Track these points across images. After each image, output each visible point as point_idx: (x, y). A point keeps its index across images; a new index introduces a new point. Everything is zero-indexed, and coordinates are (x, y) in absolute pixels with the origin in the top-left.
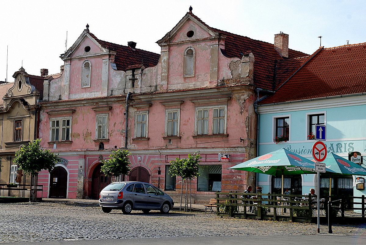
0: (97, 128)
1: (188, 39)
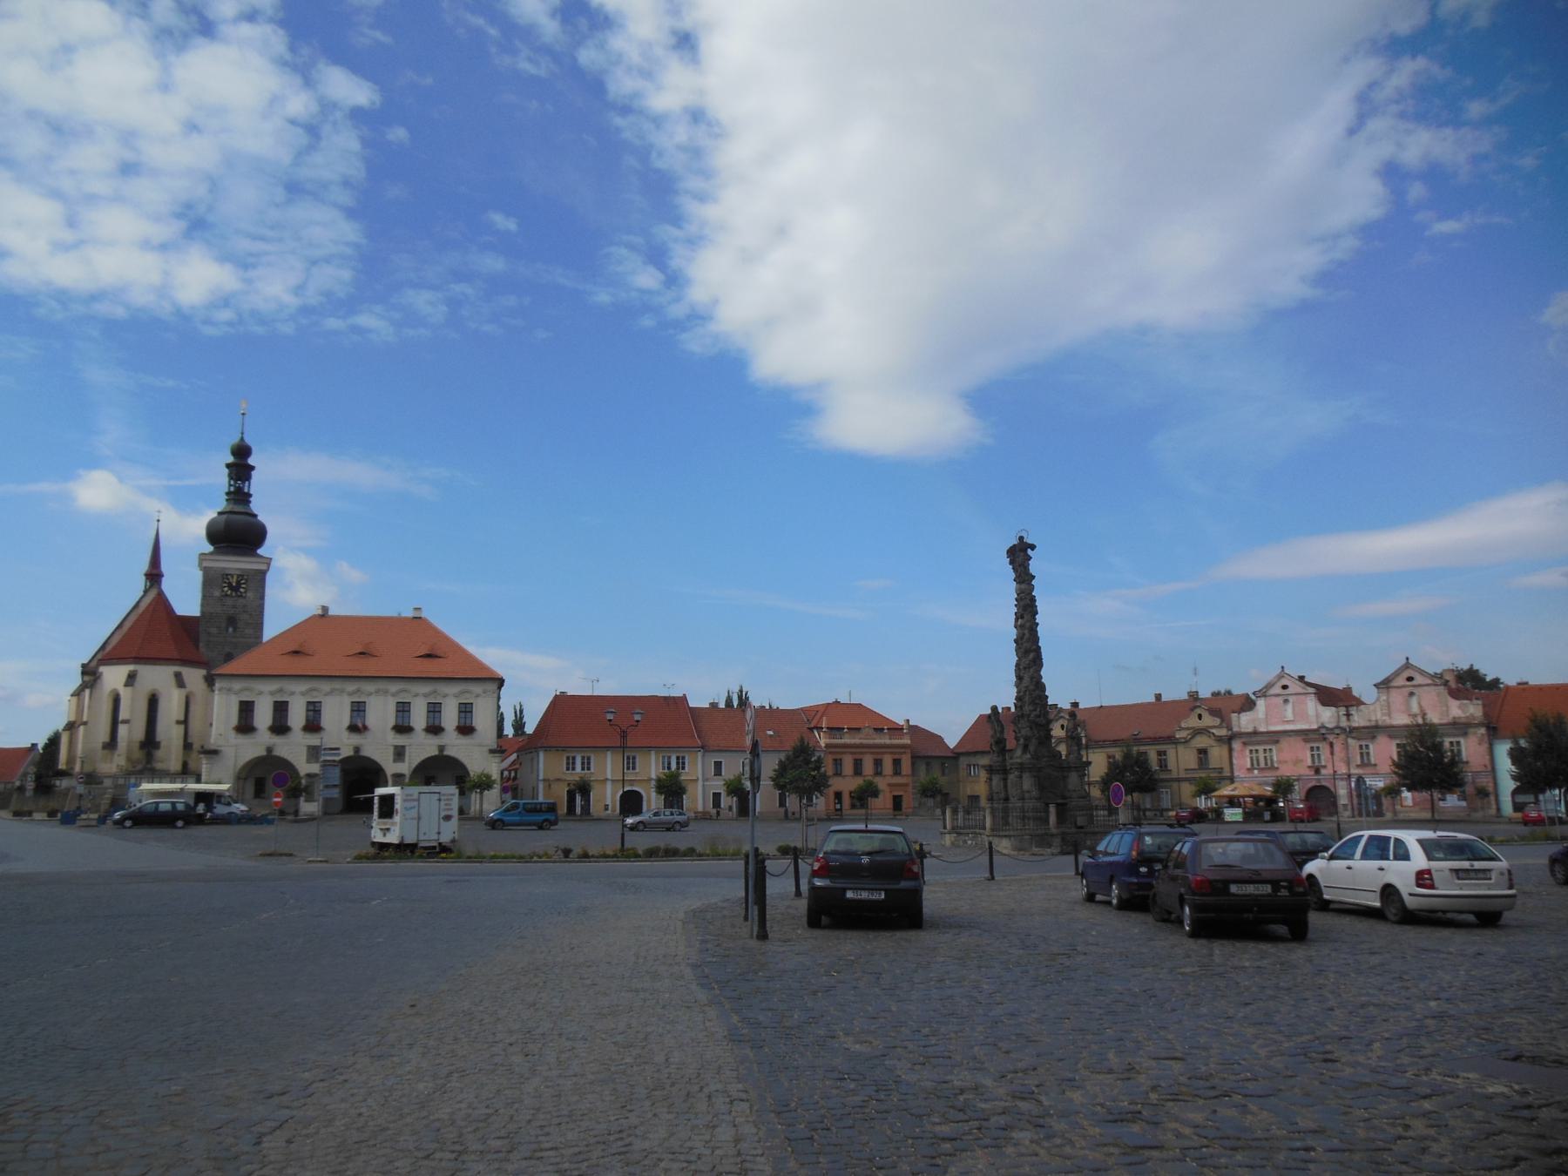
1: (1408, 683)
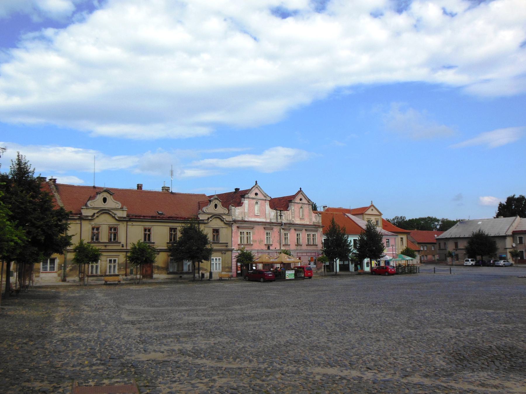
0: (266, 238)
1: (300, 202)
